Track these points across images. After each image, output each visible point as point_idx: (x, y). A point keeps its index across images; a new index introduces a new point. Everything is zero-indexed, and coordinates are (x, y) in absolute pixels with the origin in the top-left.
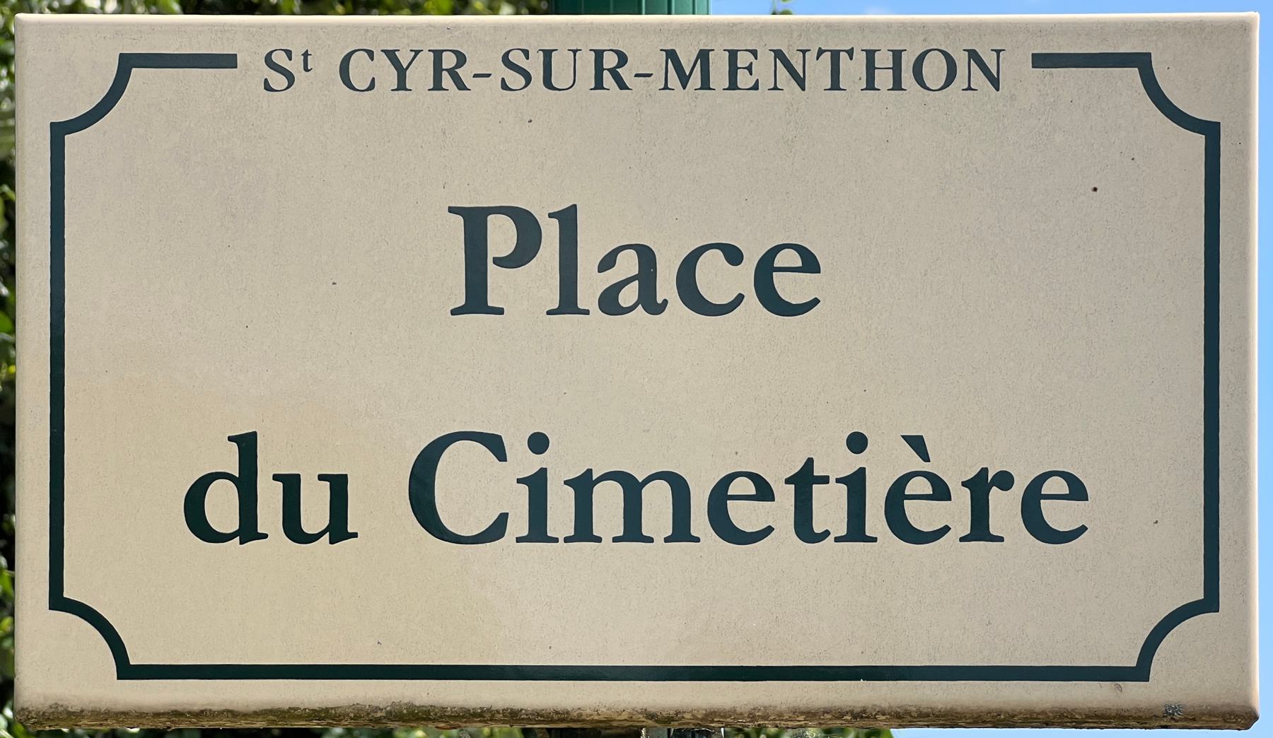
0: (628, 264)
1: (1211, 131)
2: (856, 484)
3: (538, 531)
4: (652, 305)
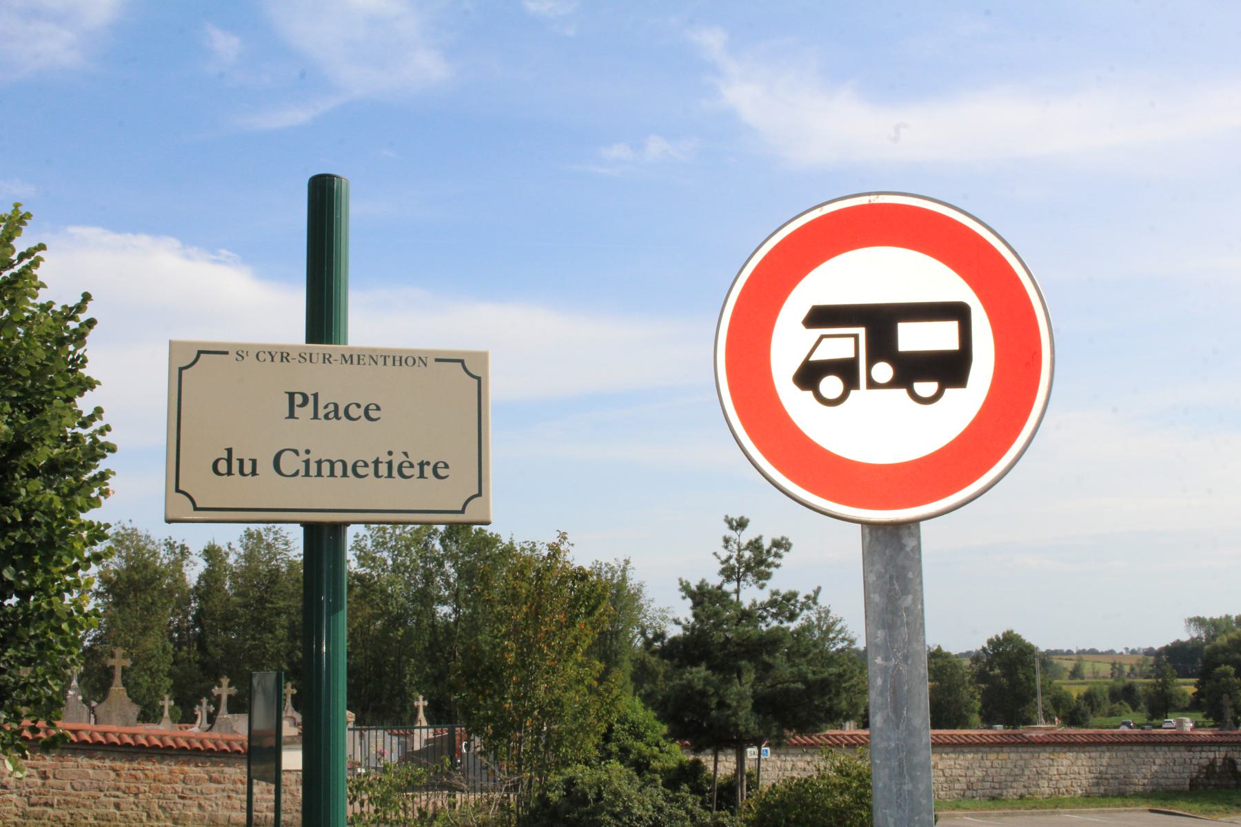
0: (331, 407)
1: (479, 379)
2: (390, 464)
3: (307, 474)
4: (337, 417)
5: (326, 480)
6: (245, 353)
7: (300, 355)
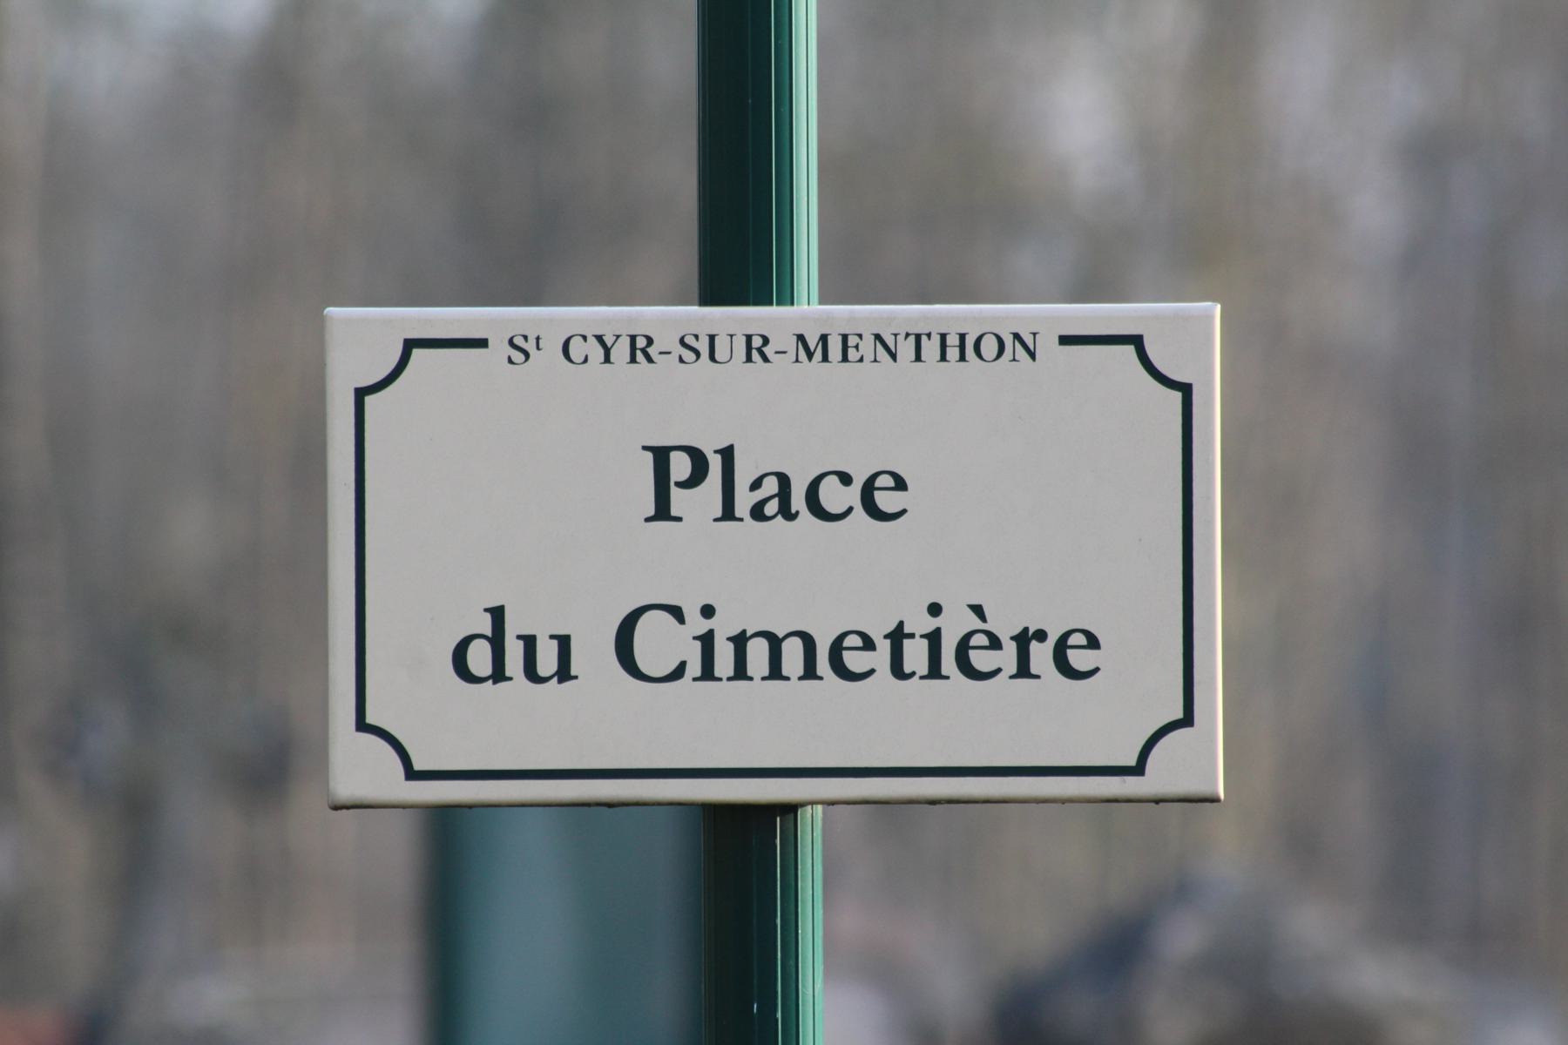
0: (771, 486)
4: (787, 513)
5: (759, 689)
6: (532, 341)
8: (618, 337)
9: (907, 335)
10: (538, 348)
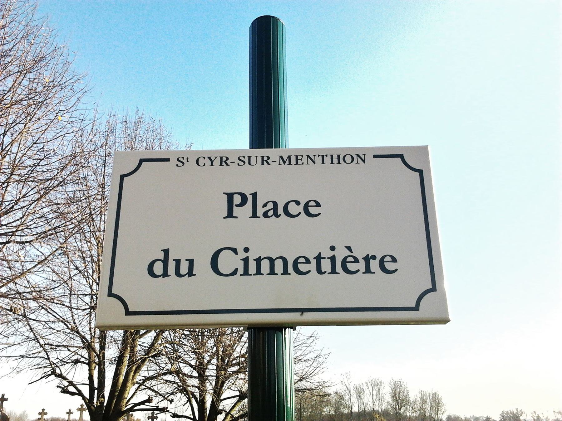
0: (270, 206)
1: (421, 172)
3: (246, 272)
4: (276, 215)
5: (265, 279)
6: (185, 159)
7: (239, 159)
8: (216, 157)
9: (319, 156)
10: (187, 161)
